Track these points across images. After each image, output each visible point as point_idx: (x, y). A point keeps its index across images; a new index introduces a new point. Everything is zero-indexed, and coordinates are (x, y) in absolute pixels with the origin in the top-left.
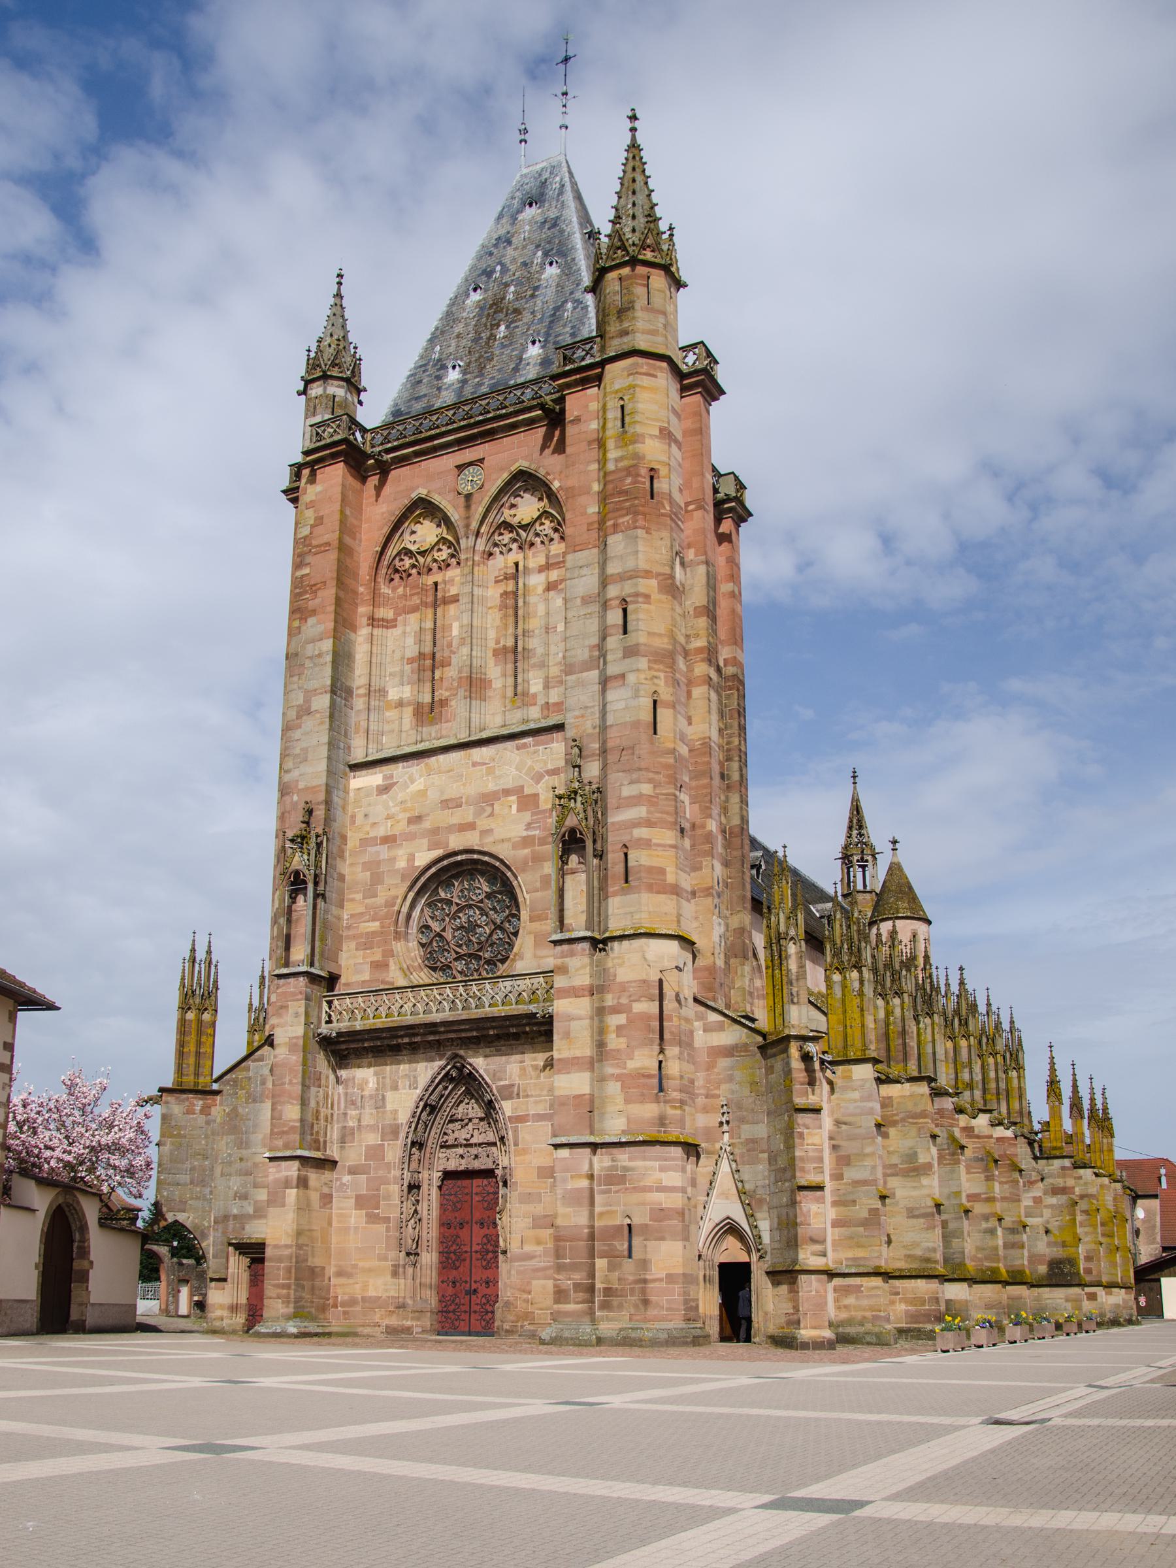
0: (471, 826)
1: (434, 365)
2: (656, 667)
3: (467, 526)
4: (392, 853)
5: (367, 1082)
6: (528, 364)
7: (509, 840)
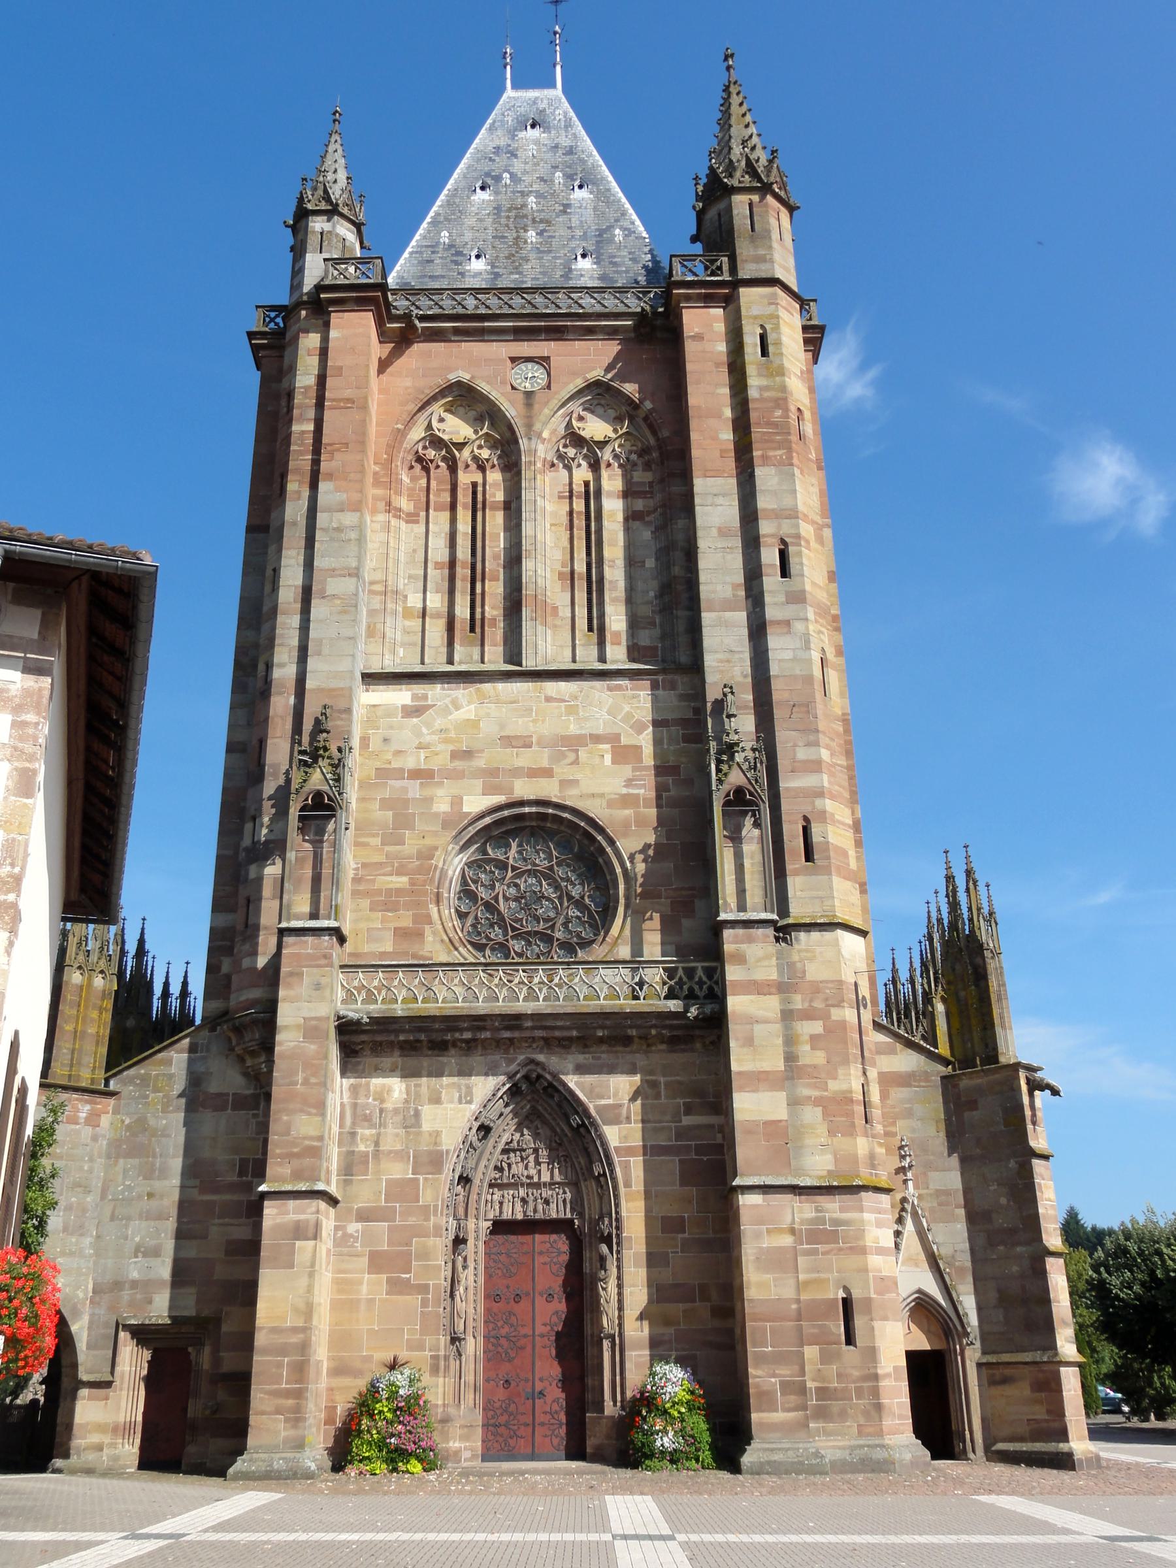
7: (602, 795)
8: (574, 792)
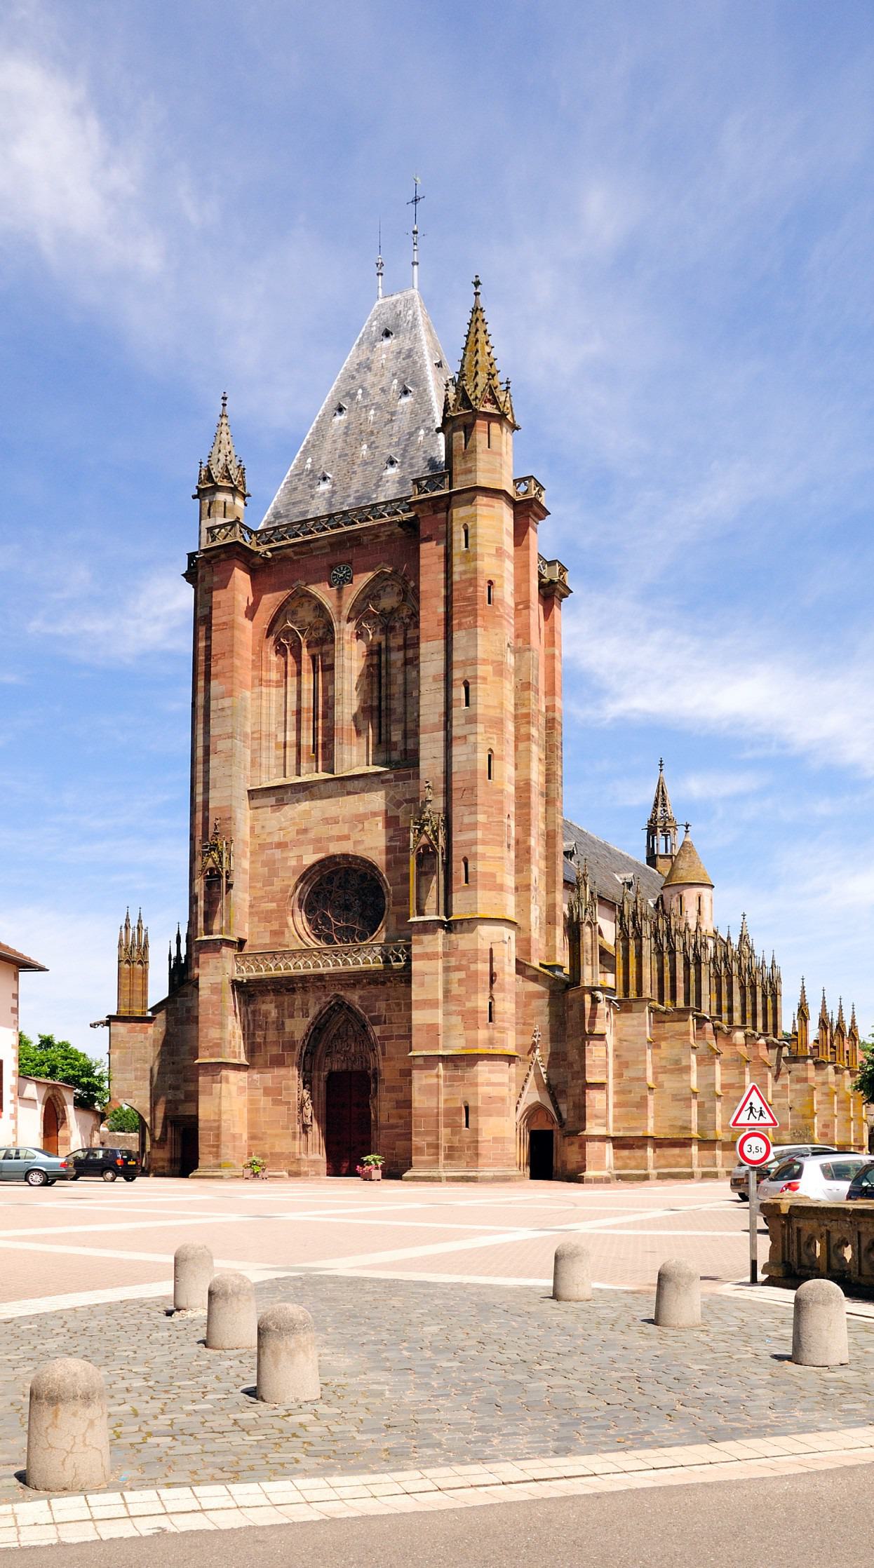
0: (347, 838)
1: (308, 475)
2: (491, 730)
3: (340, 613)
4: (284, 855)
5: (270, 1013)
6: (387, 481)
7: (376, 848)
8: (361, 847)
